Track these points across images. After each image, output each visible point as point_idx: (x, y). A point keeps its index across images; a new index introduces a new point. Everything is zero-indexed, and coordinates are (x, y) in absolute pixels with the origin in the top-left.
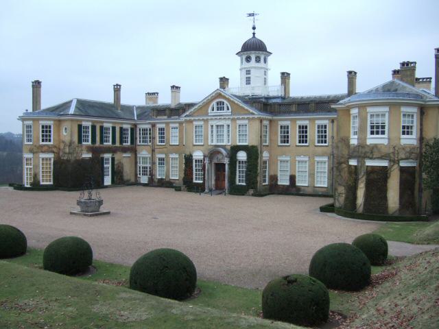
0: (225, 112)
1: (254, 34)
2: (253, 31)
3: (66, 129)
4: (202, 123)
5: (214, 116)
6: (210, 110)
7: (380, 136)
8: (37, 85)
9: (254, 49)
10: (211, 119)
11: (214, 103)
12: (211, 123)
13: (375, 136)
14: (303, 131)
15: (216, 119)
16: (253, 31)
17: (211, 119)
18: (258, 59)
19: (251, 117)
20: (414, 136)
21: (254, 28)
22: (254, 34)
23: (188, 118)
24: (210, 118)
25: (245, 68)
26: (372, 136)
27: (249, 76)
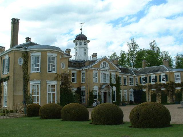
0: (106, 68)
1: (81, 32)
2: (81, 31)
3: (63, 64)
4: (97, 72)
5: (104, 69)
6: (100, 67)
8: (15, 22)
9: (81, 39)
11: (102, 62)
15: (105, 71)
16: (81, 31)
17: (101, 70)
19: (116, 71)
20: (180, 80)
21: (81, 30)
22: (81, 32)
25: (84, 48)
27: (85, 51)
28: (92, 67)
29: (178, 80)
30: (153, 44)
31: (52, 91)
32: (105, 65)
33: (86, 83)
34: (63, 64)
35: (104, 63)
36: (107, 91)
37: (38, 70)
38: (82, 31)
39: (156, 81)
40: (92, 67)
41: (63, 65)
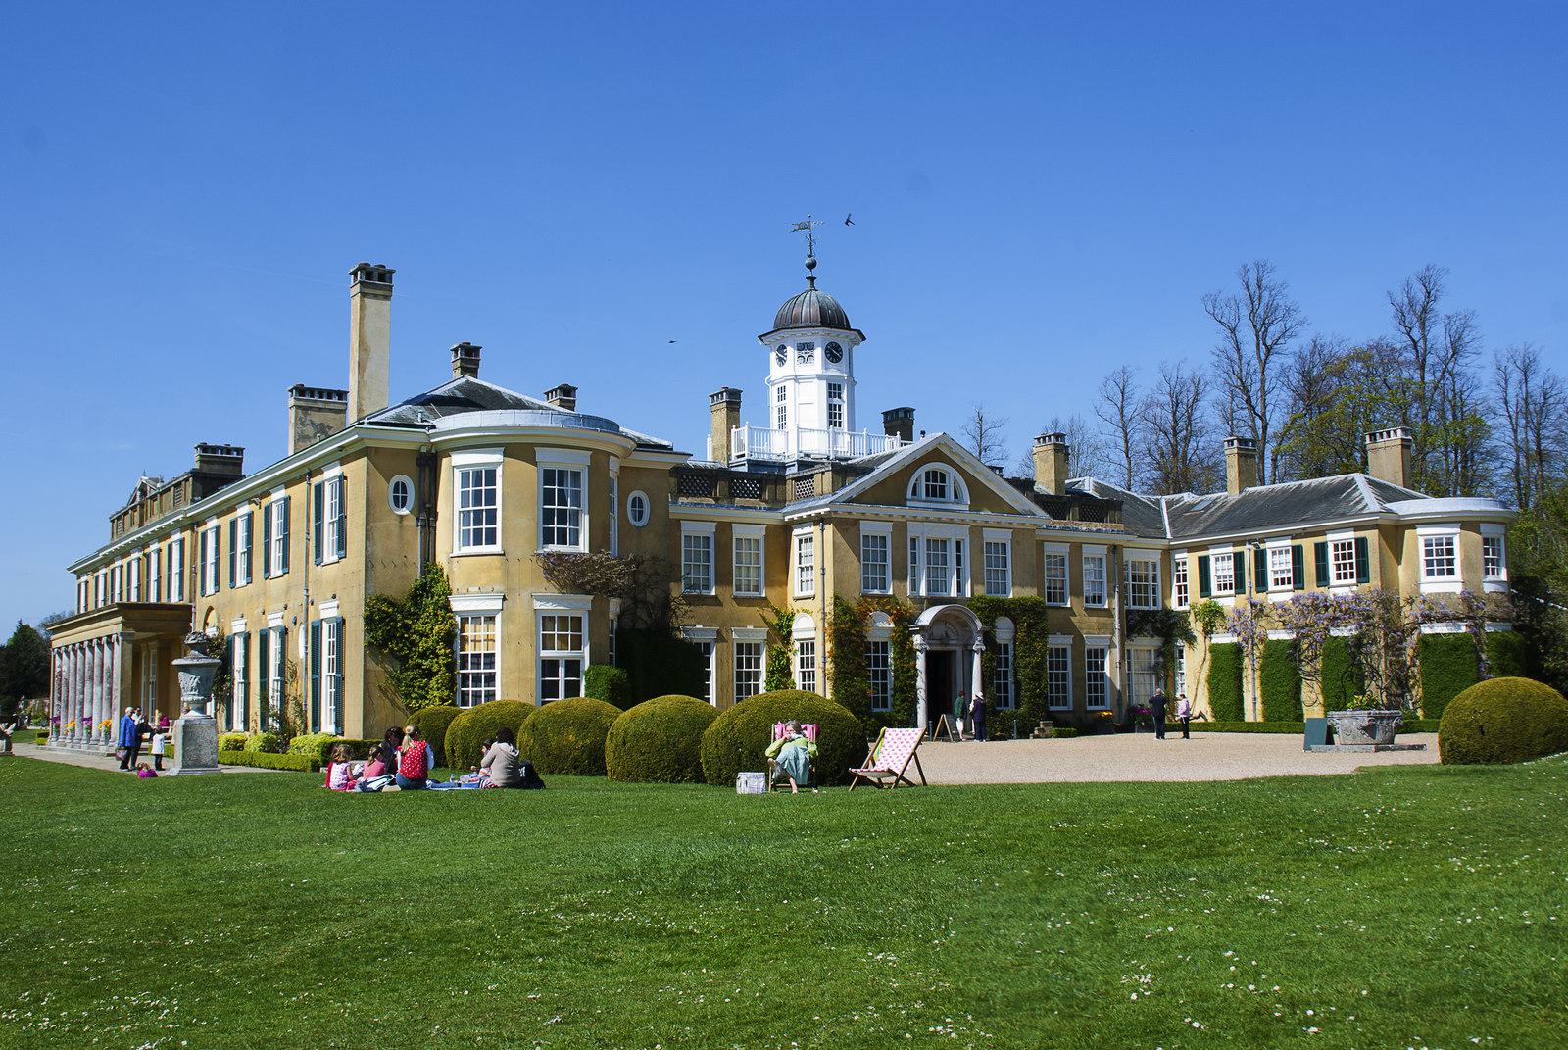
6: (909, 495)
7: (1446, 578)
10: (915, 519)
11: (921, 472)
12: (913, 530)
13: (1436, 578)
14: (1345, 568)
17: (915, 519)
18: (833, 354)
21: (812, 266)
22: (812, 279)
23: (857, 509)
24: (913, 512)
26: (1431, 579)
28: (850, 501)
29: (1441, 573)
30: (1420, 295)
31: (564, 645)
32: (942, 489)
33: (819, 597)
34: (638, 503)
35: (932, 476)
36: (954, 645)
37: (491, 540)
38: (815, 272)
39: (1298, 580)
40: (850, 501)
41: (641, 506)
